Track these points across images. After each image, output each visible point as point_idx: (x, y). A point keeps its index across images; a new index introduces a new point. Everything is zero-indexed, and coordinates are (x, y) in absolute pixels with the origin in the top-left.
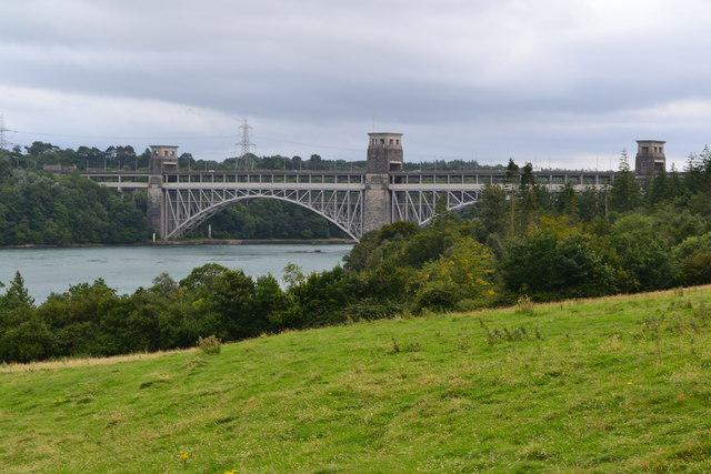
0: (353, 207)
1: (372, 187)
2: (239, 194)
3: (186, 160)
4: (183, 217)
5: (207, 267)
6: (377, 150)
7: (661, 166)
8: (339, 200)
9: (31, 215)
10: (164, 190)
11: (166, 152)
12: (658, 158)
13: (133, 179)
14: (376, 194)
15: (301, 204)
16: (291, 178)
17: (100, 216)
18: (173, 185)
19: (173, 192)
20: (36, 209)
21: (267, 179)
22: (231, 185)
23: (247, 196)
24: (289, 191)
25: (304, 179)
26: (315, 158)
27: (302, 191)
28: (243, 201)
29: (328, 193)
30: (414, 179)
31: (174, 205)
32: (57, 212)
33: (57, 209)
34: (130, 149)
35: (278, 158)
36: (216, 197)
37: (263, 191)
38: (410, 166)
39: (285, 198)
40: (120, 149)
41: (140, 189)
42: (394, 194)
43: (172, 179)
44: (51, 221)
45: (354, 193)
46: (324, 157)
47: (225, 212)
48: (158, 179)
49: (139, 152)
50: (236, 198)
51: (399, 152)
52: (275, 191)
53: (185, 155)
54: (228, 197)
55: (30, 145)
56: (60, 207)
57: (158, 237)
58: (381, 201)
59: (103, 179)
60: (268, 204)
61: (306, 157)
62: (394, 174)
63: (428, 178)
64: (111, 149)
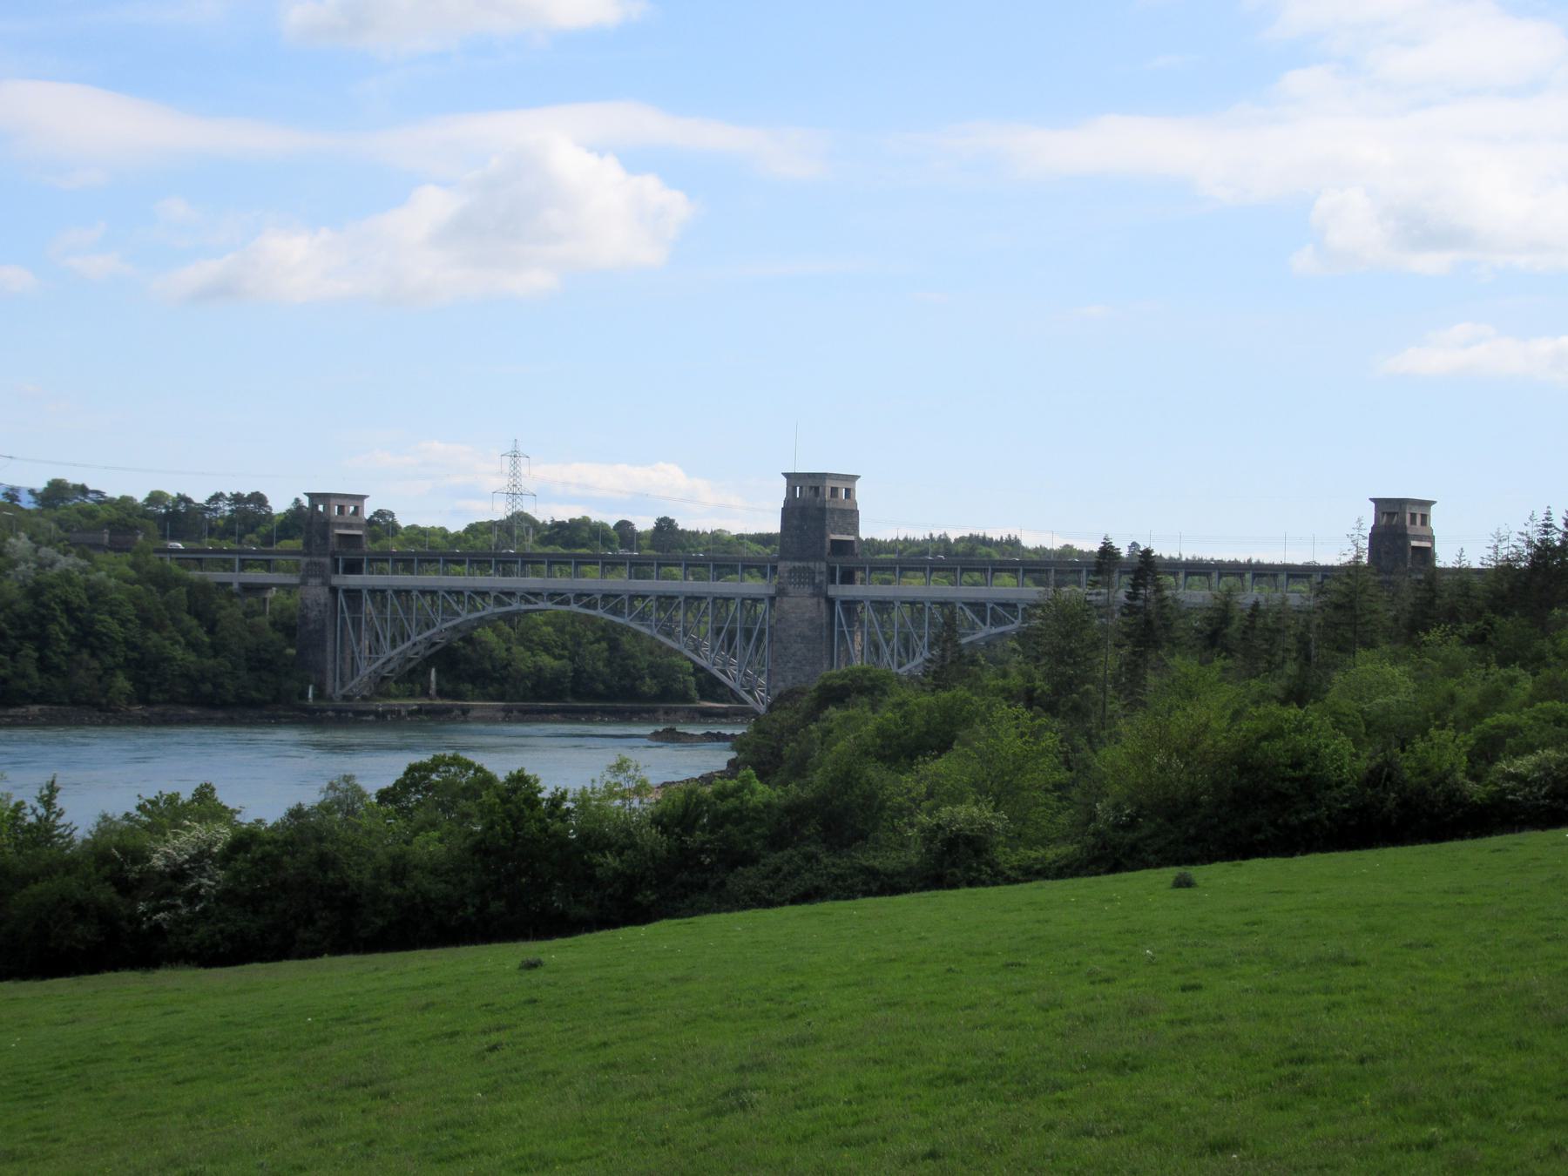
1: (790, 588)
3: (383, 524)
4: (375, 649)
7: (1427, 554)
9: (43, 641)
10: (334, 590)
11: (341, 509)
12: (1420, 538)
14: (802, 605)
17: (193, 645)
18: (353, 580)
19: (353, 595)
20: (54, 628)
23: (516, 605)
24: (607, 597)
28: (508, 618)
33: (98, 627)
34: (259, 499)
35: (583, 523)
37: (552, 596)
40: (237, 498)
42: (838, 607)
43: (353, 567)
49: (279, 504)
51: (850, 517)
52: (579, 596)
55: (40, 485)
56: (107, 624)
57: (320, 694)
62: (839, 563)
64: (217, 497)
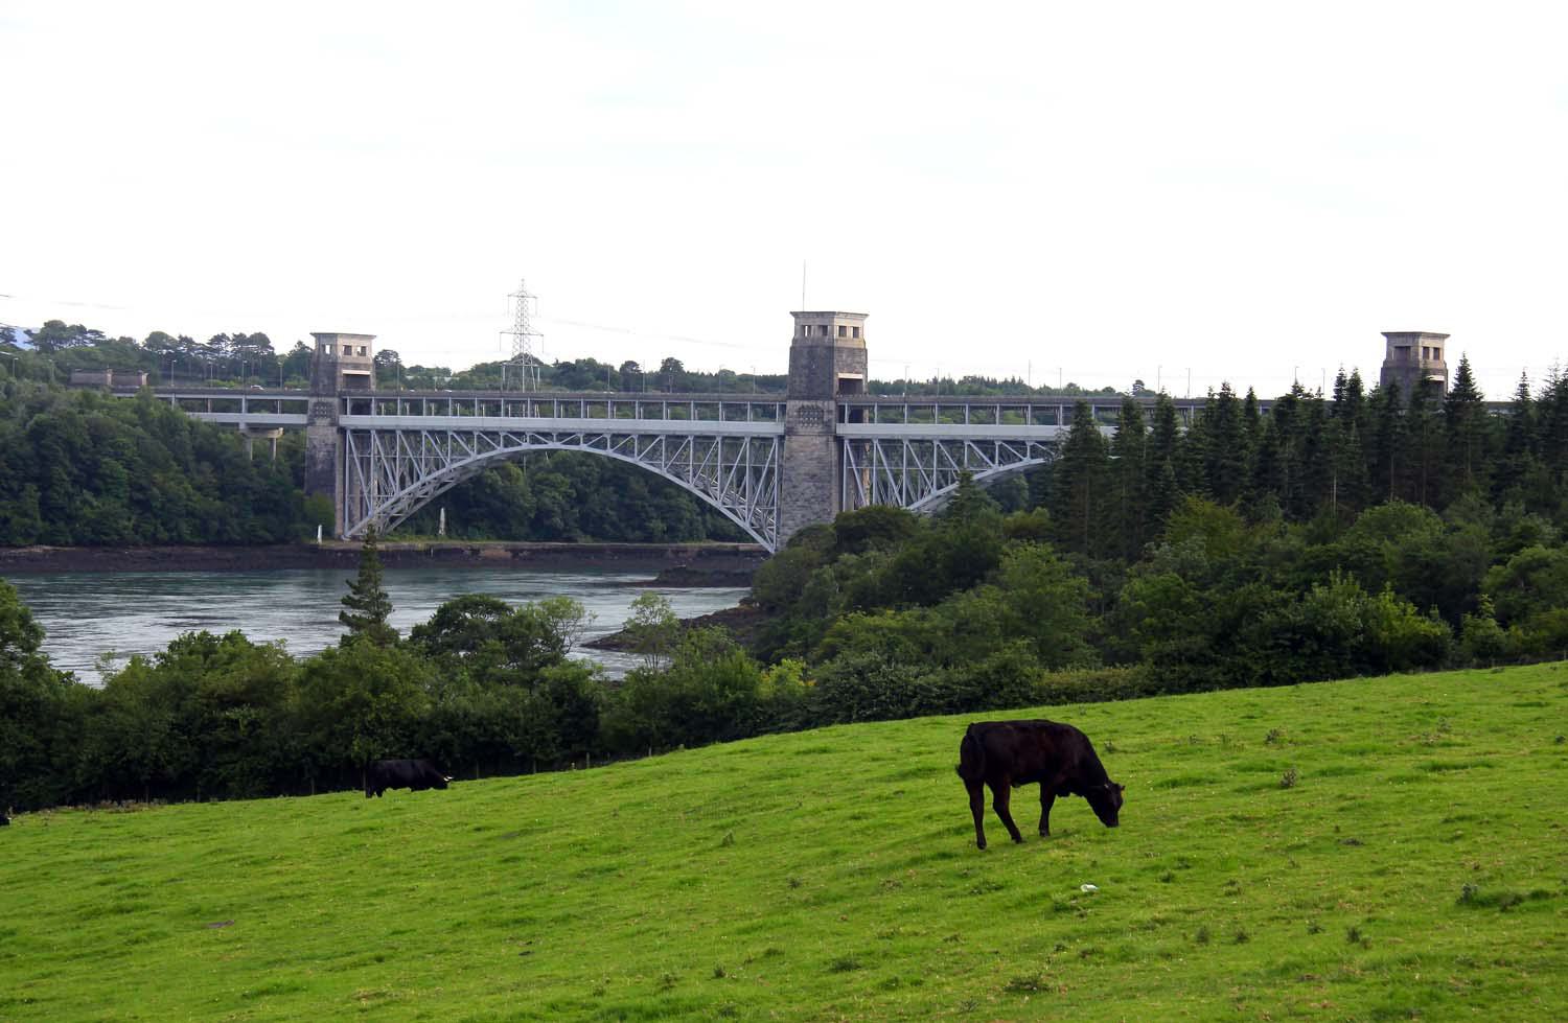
0: (757, 472)
1: (800, 429)
2: (508, 443)
3: (388, 367)
6: (812, 349)
8: (725, 459)
9: (45, 483)
10: (342, 431)
11: (348, 349)
13: (271, 407)
14: (810, 444)
15: (643, 464)
16: (624, 409)
19: (362, 435)
20: (58, 470)
21: (571, 409)
22: (491, 423)
23: (526, 446)
25: (652, 412)
26: (671, 365)
27: (647, 437)
28: (516, 459)
29: (704, 441)
30: (890, 414)
31: (365, 463)
32: (103, 477)
34: (261, 340)
37: (562, 436)
38: (878, 388)
40: (240, 339)
41: (288, 428)
43: (361, 408)
45: (763, 442)
46: (689, 366)
47: (477, 481)
48: (329, 405)
49: (282, 347)
50: (500, 450)
51: (859, 355)
52: (589, 436)
53: (385, 354)
58: (819, 459)
59: (202, 406)
62: (847, 402)
63: (920, 413)
64: (219, 339)
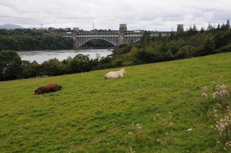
0: (116, 40)
4: (80, 43)
5: (79, 55)
7: (183, 30)
10: (76, 37)
14: (121, 38)
16: (103, 34)
18: (78, 36)
19: (78, 38)
23: (94, 38)
24: (103, 37)
29: (111, 37)
30: (129, 34)
31: (79, 40)
34: (70, 28)
36: (87, 39)
39: (102, 39)
40: (68, 28)
44: (52, 44)
45: (117, 37)
47: (90, 42)
50: (92, 39)
51: (126, 28)
52: (100, 37)
54: (90, 38)
55: (49, 28)
57: (75, 47)
60: (98, 40)
61: (107, 30)
62: (125, 33)
64: (66, 28)
